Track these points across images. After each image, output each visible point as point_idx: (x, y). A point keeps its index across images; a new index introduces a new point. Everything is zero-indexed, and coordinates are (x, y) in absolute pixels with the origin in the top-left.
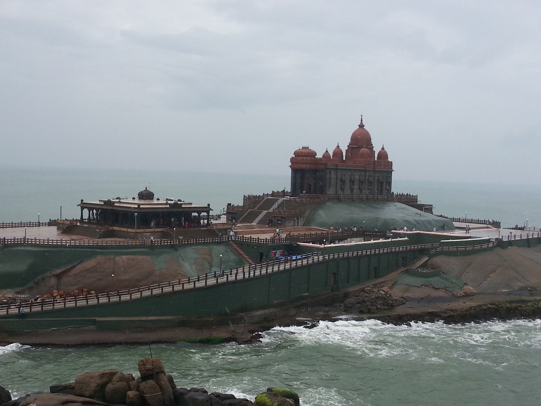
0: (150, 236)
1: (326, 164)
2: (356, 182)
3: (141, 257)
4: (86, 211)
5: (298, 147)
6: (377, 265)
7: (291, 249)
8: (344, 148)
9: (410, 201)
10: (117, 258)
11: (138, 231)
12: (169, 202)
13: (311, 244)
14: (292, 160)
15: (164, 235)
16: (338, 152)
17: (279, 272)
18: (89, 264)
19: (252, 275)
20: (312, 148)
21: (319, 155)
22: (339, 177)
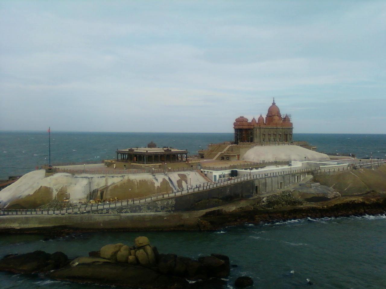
5: (238, 116)
8: (264, 116)
12: (164, 149)
13: (243, 170)
14: (235, 124)
16: (261, 119)
20: (246, 116)
21: (250, 121)
22: (262, 132)
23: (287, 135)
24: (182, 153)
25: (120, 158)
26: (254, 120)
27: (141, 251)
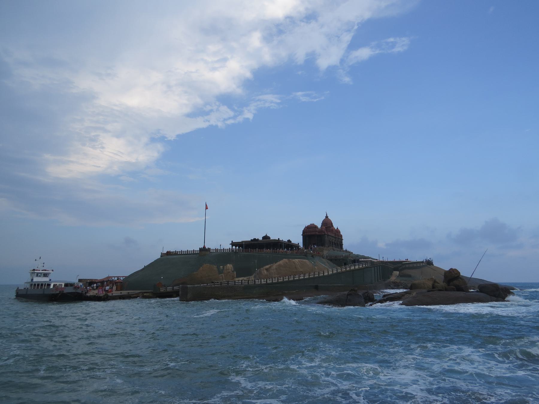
10: (294, 260)
18: (281, 262)
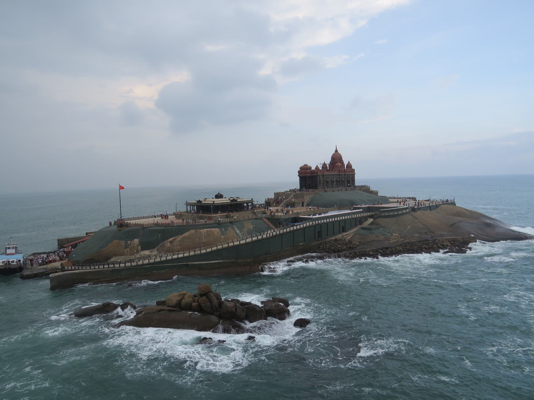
0: (219, 216)
1: (317, 173)
2: (335, 181)
3: (213, 229)
4: (189, 207)
5: (302, 165)
6: (343, 225)
7: (296, 220)
9: (365, 189)
10: (202, 231)
11: (213, 215)
14: (299, 172)
15: (227, 217)
16: (324, 165)
17: (287, 233)
18: (187, 234)
19: (271, 235)
21: (313, 168)
23: (349, 181)
24: (247, 203)
25: (189, 210)
26: (317, 168)
27: (204, 297)
